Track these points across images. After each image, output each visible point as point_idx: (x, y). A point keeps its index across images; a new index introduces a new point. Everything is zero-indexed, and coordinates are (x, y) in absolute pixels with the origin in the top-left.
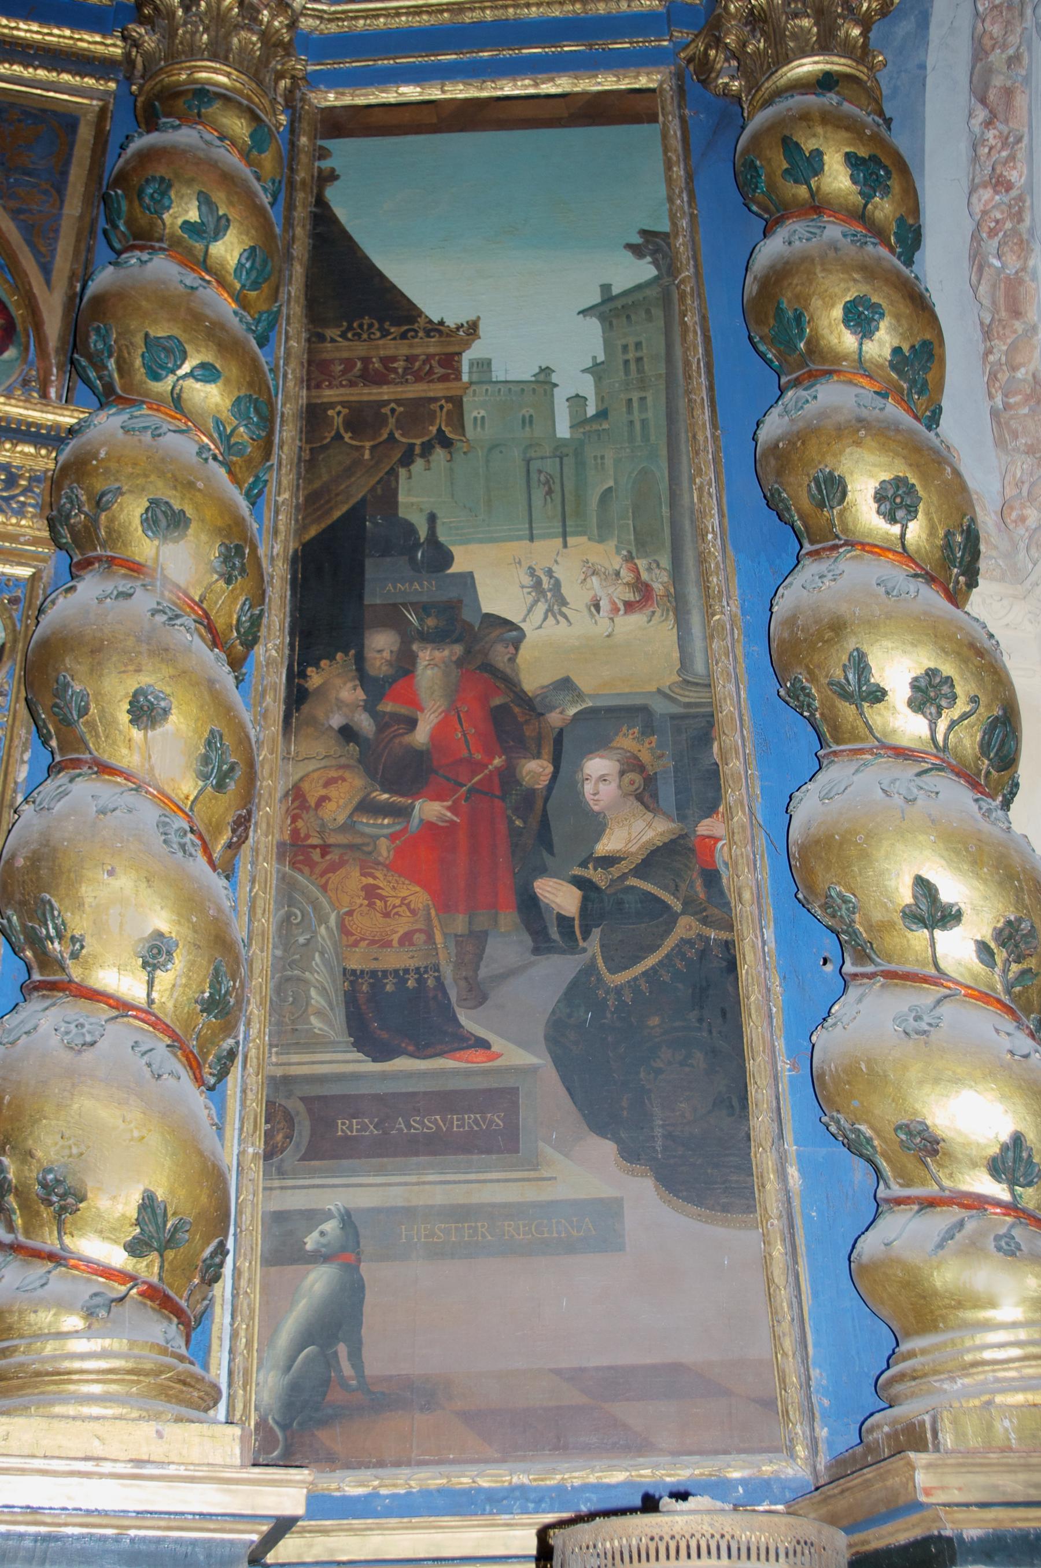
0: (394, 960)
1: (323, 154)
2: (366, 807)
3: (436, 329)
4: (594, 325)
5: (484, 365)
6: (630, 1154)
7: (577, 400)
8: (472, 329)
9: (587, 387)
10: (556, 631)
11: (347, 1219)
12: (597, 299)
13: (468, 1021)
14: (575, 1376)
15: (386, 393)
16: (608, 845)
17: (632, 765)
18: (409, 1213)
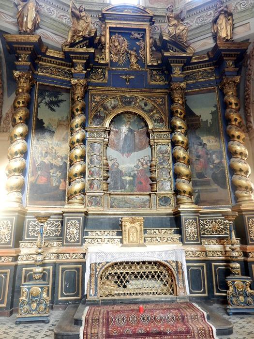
0: (200, 171)
1: (185, 98)
2: (196, 160)
3: (197, 116)
4: (211, 115)
5: (202, 120)
6: (218, 185)
7: (210, 123)
8: (200, 116)
9: (211, 121)
10: (210, 144)
11: (198, 190)
12: (211, 112)
13: (205, 176)
14: (215, 200)
15: (194, 123)
16: (215, 162)
17: (216, 155)
18: (203, 190)
